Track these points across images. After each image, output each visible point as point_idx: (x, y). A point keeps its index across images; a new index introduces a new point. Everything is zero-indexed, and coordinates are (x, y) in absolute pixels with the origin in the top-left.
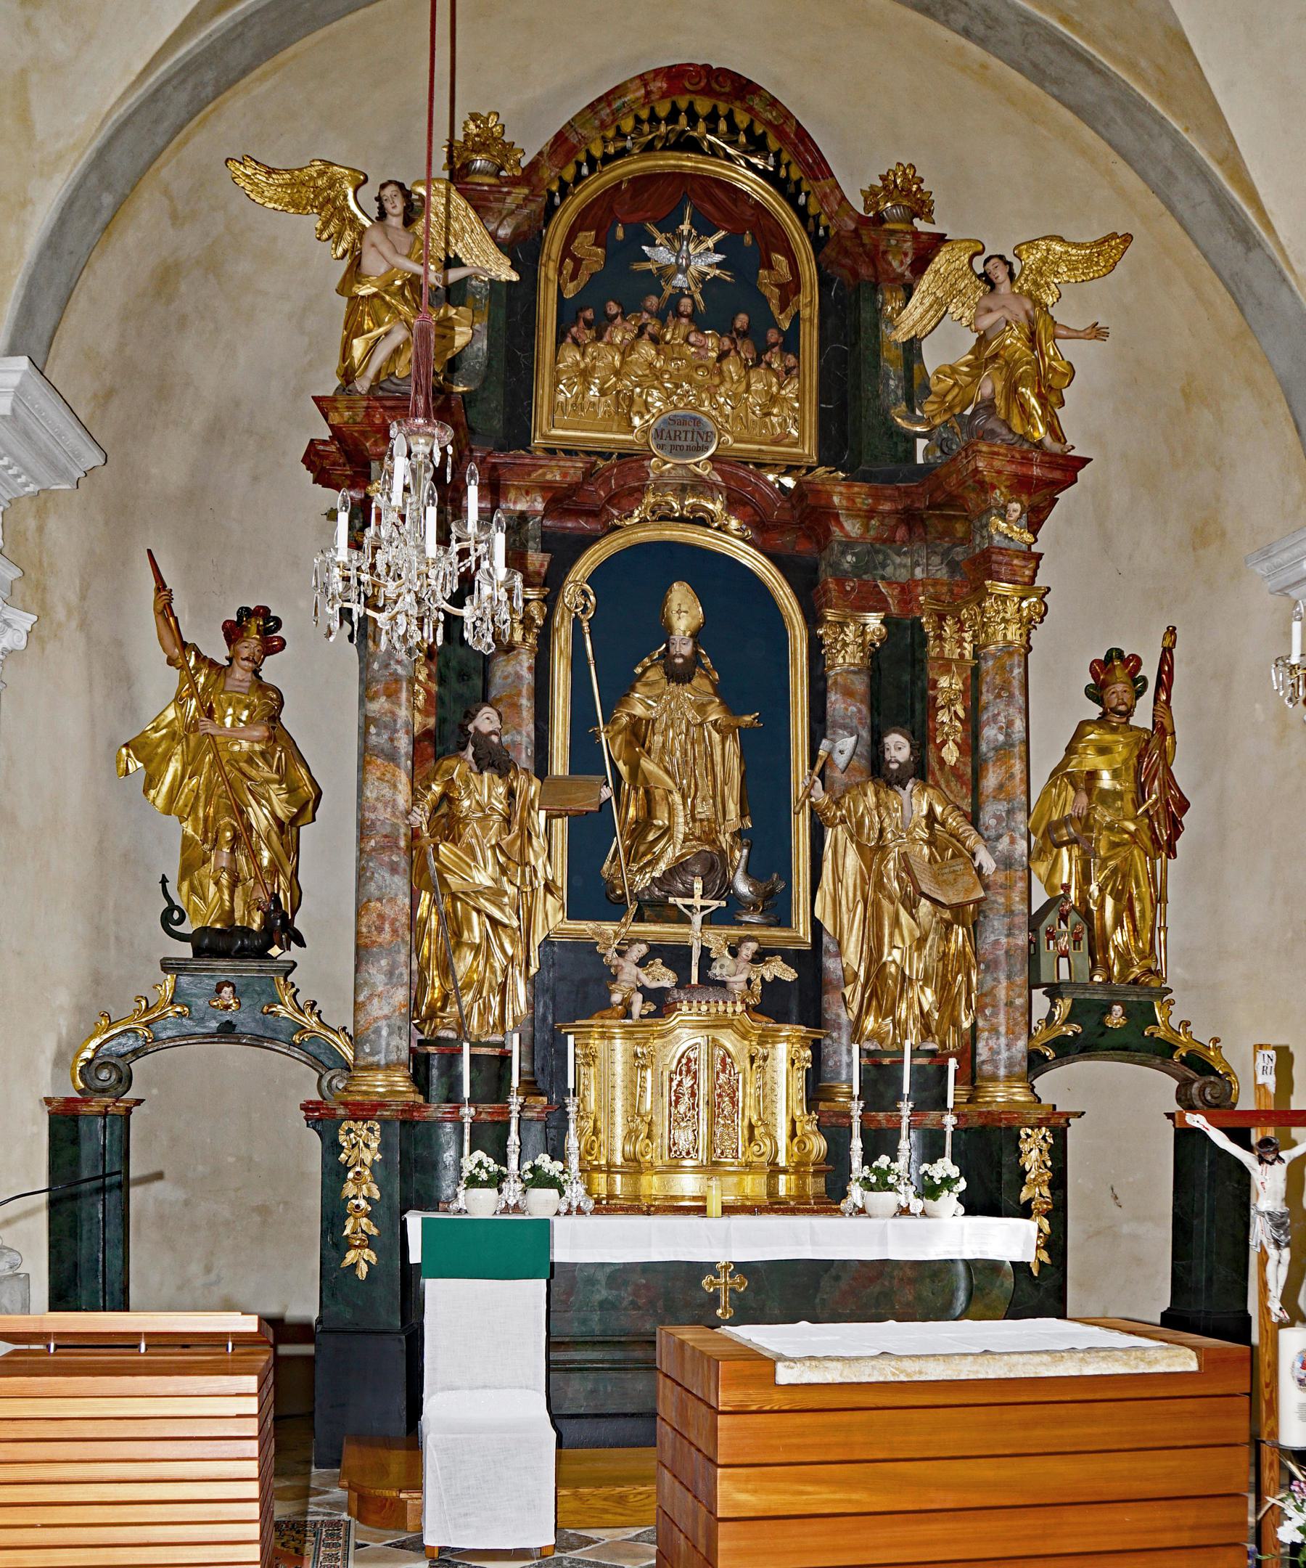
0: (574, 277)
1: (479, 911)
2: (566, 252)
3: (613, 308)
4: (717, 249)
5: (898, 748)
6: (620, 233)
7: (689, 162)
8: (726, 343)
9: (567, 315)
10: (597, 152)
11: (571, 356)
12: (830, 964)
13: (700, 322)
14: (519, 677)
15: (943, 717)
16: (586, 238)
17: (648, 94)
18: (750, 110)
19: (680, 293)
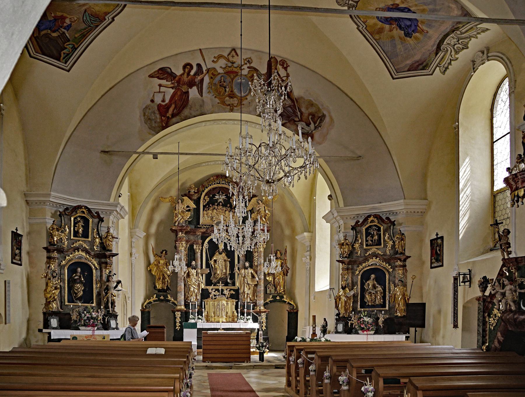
0: (205, 202)
1: (193, 287)
2: (204, 199)
3: (211, 205)
4: (225, 196)
5: (247, 264)
6: (211, 196)
7: (220, 185)
8: (226, 209)
9: (204, 207)
10: (207, 186)
11: (205, 212)
12: (240, 291)
13: (223, 205)
14: (198, 256)
15: (255, 259)
16: (206, 197)
17: (214, 179)
18: (228, 179)
19: (221, 202)
